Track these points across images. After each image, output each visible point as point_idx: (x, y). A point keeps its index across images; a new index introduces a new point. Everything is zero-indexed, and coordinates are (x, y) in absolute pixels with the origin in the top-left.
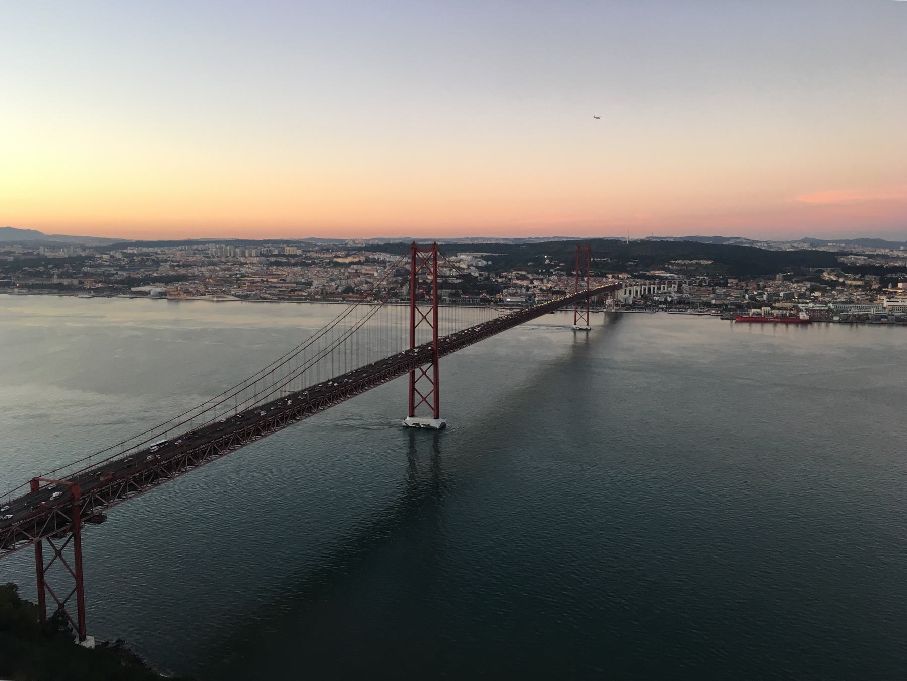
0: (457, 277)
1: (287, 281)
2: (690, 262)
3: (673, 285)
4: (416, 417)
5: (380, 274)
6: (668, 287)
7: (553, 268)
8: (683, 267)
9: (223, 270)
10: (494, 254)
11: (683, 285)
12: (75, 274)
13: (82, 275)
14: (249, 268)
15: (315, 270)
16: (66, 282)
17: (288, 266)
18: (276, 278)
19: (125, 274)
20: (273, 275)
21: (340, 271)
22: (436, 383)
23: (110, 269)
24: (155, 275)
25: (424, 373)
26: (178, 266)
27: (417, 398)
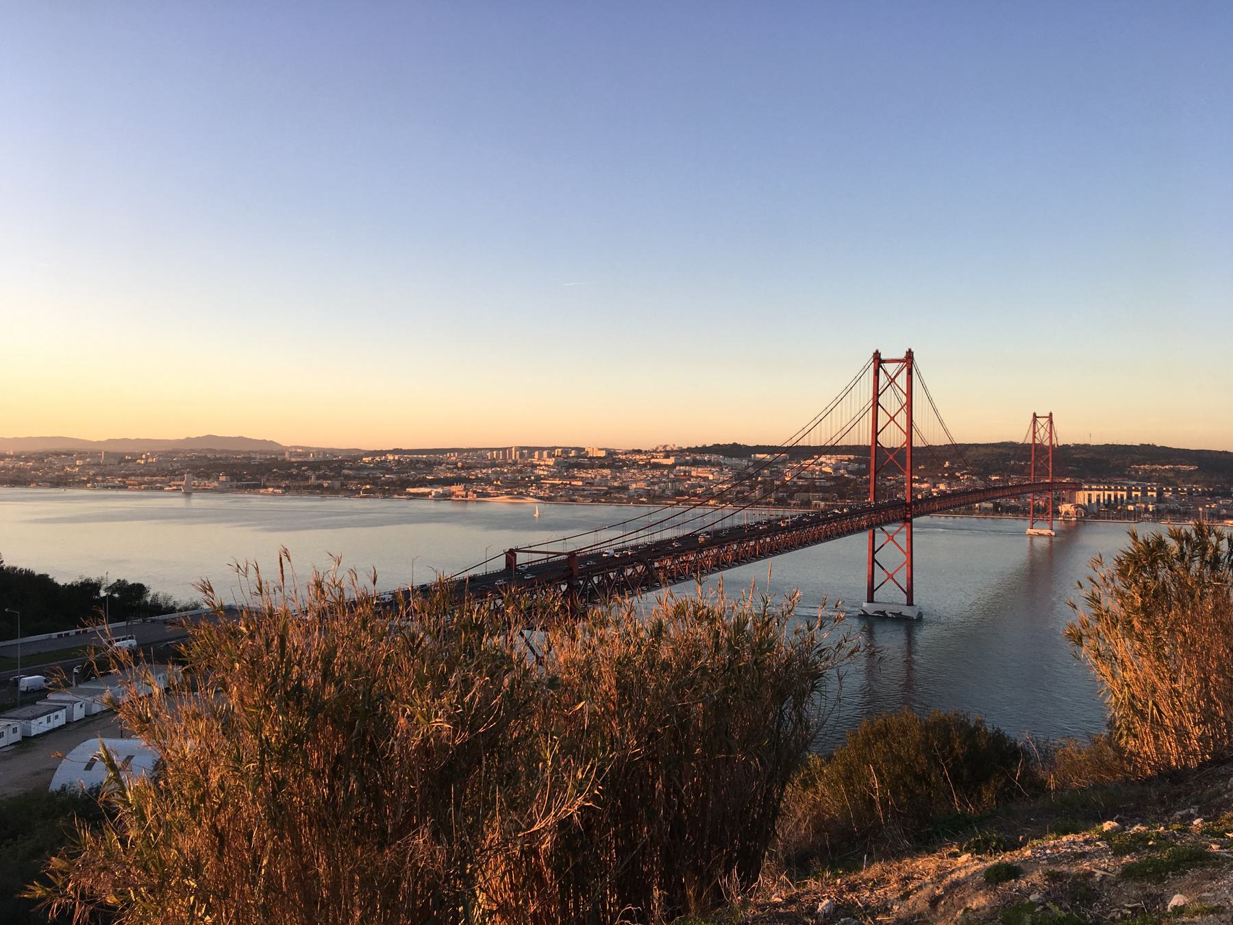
1: (595, 484)
2: (1162, 468)
3: (1149, 494)
4: (876, 602)
6: (1142, 496)
7: (959, 472)
9: (513, 472)
12: (333, 476)
13: (342, 478)
14: (543, 470)
17: (593, 468)
18: (579, 481)
20: (574, 478)
21: (662, 473)
23: (374, 472)
24: (429, 478)
25: (891, 538)
26: (458, 468)
27: (879, 576)
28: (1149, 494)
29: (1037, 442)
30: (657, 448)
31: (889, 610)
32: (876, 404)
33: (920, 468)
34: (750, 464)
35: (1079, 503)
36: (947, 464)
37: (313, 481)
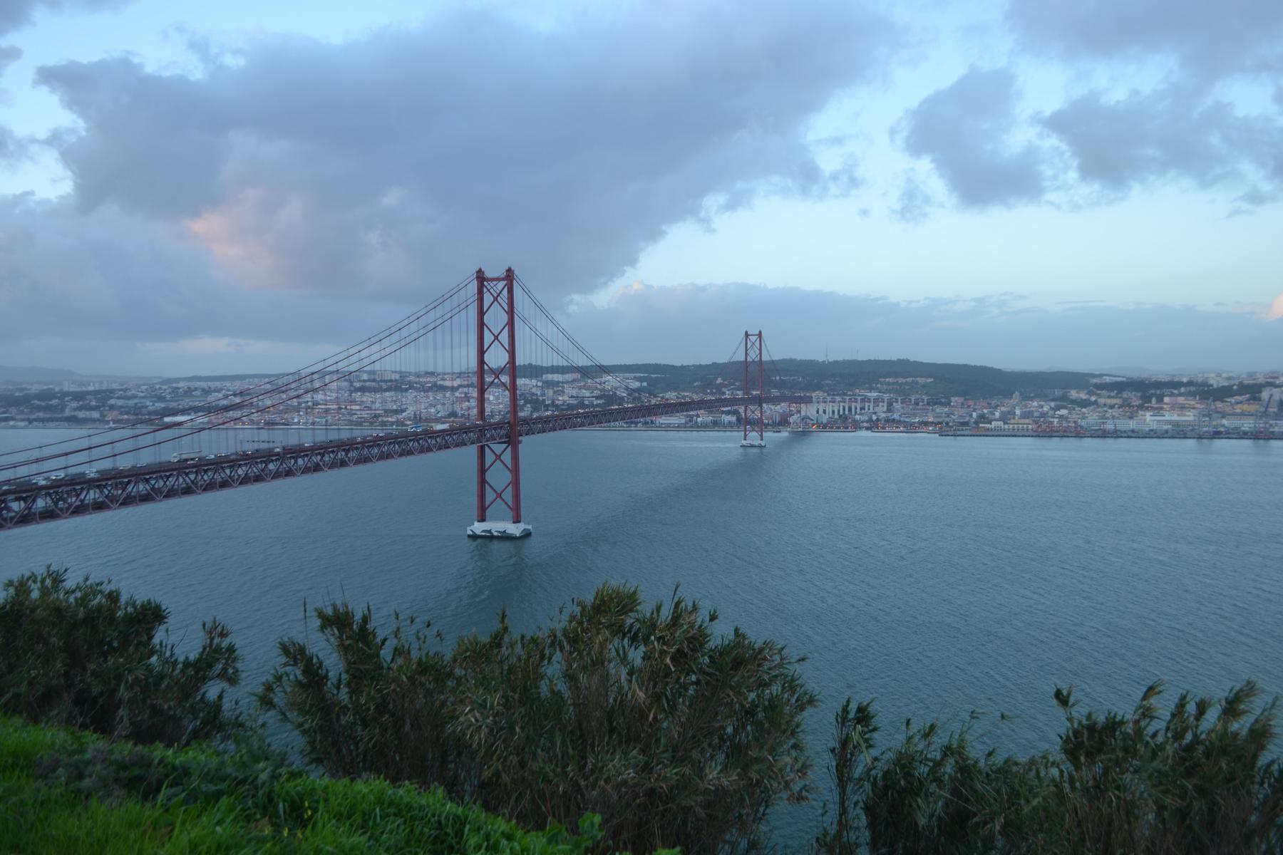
0: (597, 398)
2: (904, 381)
3: (881, 404)
5: (498, 398)
8: (895, 387)
10: (653, 375)
11: (894, 404)
13: (107, 408)
15: (411, 395)
16: (81, 414)
19: (163, 405)
22: (515, 471)
25: (498, 457)
26: (235, 395)
27: (490, 496)
28: (881, 404)
29: (749, 359)
30: (468, 368)
31: (496, 526)
32: (481, 325)
33: (695, 384)
34: (540, 384)
35: (808, 414)
36: (719, 380)
37: (67, 413)
